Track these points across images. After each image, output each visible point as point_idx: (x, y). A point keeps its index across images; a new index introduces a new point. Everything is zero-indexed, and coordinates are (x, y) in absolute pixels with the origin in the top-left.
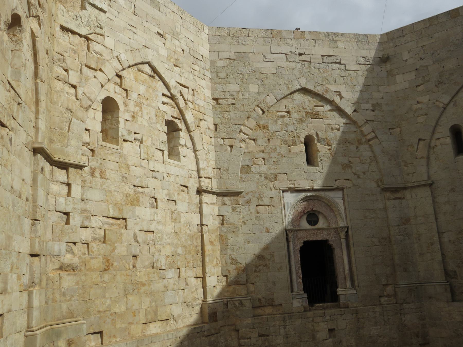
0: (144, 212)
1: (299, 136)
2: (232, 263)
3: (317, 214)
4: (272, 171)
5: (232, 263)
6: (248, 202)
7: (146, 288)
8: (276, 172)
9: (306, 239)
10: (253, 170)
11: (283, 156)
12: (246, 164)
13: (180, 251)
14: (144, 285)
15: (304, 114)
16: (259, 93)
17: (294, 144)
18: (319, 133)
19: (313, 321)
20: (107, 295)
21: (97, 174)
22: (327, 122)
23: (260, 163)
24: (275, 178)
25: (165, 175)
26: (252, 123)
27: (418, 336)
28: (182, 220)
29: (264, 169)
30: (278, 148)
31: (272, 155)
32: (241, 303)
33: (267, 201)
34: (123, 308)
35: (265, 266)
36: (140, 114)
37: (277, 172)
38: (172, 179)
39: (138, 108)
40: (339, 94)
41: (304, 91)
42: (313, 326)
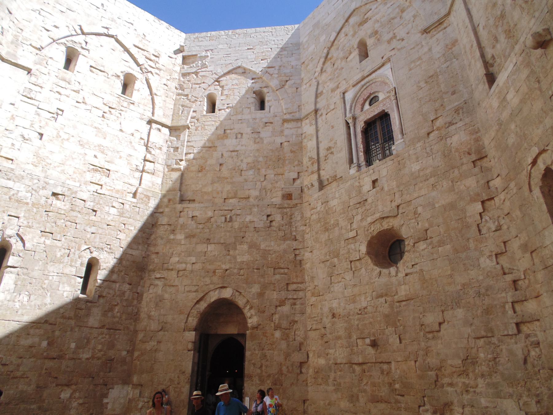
0: (231, 143)
1: (353, 47)
2: (309, 161)
3: (376, 94)
5: (309, 161)
6: (321, 115)
7: (229, 180)
8: (338, 83)
9: (365, 119)
10: (324, 91)
11: (342, 68)
13: (261, 159)
14: (227, 178)
19: (359, 179)
20: (200, 183)
21: (199, 128)
25: (251, 120)
27: (469, 154)
28: (265, 142)
32: (312, 185)
33: (332, 107)
34: (210, 190)
35: (332, 153)
38: (257, 121)
42: (359, 183)
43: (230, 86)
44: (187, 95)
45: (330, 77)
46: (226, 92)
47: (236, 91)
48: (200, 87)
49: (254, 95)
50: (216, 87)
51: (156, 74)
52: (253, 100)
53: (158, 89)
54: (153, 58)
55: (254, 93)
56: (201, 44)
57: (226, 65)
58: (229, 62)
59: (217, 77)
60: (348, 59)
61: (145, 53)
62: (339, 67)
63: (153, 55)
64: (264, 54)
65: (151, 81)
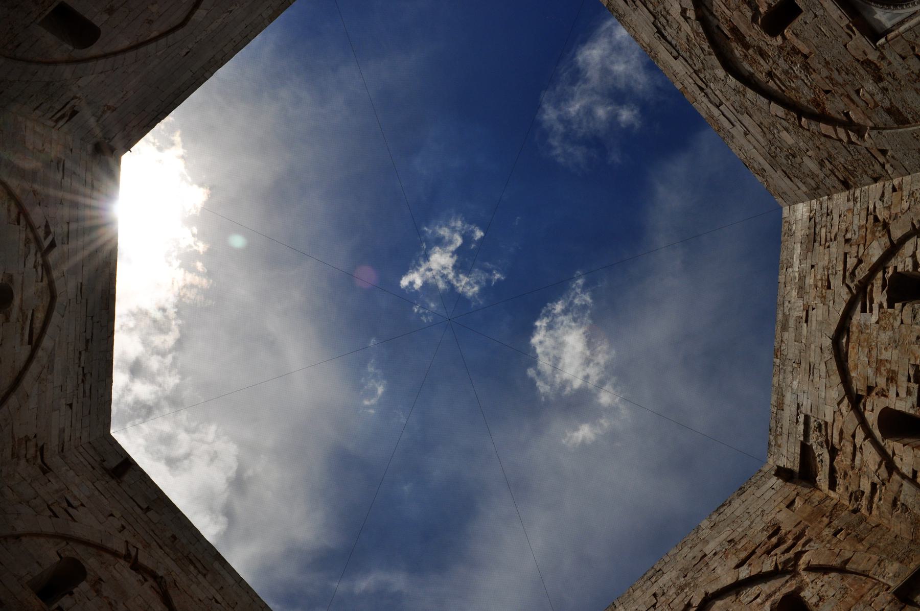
1: (781, 48)
4: (862, 71)
8: (859, 66)
10: (887, 104)
11: (827, 63)
12: (888, 117)
15: (751, 51)
16: (786, 129)
17: (796, 51)
18: (749, 18)
22: (726, 11)
23: (868, 96)
24: (867, 63)
26: (825, 128)
29: (870, 86)
30: (824, 75)
31: (840, 80)
36: (888, 366)
37: (855, 64)
39: (883, 368)
40: (684, 12)
41: (731, 67)
43: (870, 372)
44: (874, 486)
45: (854, 97)
46: (882, 382)
47: (886, 355)
48: (861, 448)
49: (898, 305)
50: (869, 407)
51: (804, 545)
52: (908, 308)
53: (837, 551)
54: (774, 540)
55: (891, 306)
56: (785, 431)
57: (828, 375)
58: (823, 367)
59: (846, 401)
60: (806, 51)
61: (759, 552)
62: (825, 73)
63: (770, 537)
64: (819, 284)
65: (814, 562)
